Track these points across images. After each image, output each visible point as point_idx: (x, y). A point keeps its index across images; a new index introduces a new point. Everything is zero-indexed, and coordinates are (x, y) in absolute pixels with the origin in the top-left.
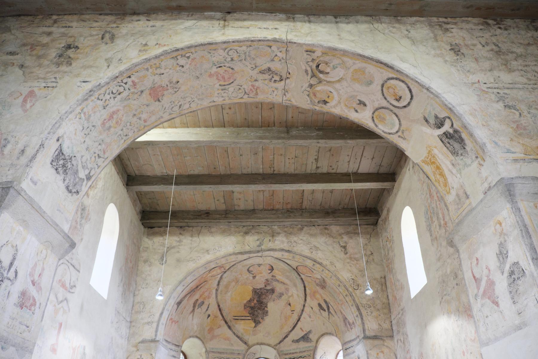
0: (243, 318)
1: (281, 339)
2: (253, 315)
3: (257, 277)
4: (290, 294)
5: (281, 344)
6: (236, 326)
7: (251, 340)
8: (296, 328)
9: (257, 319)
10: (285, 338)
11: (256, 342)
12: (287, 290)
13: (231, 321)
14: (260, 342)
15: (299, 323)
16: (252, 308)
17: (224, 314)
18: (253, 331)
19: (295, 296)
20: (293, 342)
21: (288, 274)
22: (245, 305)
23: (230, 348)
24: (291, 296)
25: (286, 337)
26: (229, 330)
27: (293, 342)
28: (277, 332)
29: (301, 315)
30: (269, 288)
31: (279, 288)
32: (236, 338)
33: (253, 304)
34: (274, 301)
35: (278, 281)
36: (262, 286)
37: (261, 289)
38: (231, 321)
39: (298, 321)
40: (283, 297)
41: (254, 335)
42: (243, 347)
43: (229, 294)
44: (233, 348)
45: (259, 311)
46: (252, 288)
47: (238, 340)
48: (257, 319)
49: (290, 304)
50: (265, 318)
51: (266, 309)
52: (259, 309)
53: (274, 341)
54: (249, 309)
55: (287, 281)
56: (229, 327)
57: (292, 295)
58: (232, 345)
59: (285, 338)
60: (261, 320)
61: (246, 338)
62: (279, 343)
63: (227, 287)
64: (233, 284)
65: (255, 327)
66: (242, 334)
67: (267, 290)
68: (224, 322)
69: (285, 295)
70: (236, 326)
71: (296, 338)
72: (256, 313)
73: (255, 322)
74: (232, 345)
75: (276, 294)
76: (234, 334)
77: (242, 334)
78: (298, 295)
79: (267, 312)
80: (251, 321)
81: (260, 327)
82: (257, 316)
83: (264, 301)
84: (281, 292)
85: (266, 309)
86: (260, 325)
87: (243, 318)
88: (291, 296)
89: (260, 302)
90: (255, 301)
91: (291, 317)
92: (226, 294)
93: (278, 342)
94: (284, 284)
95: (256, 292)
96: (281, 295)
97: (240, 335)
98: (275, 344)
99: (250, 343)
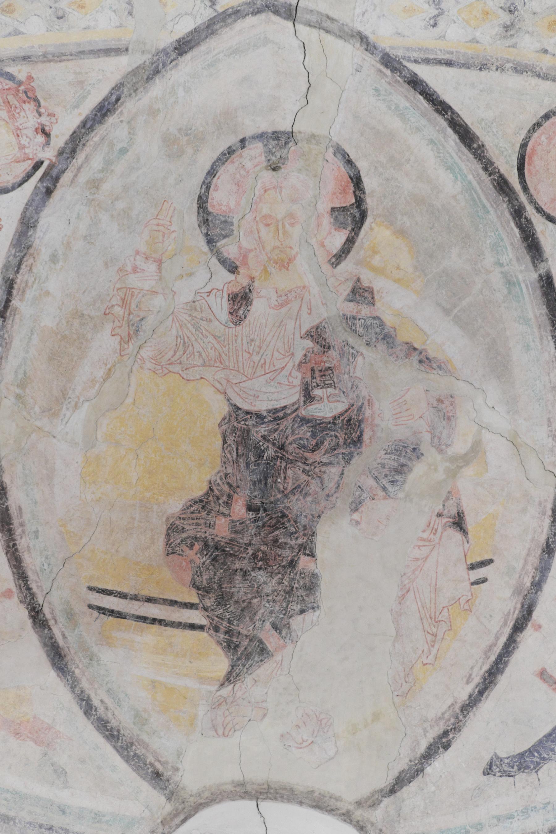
0: (153, 611)
1: (403, 764)
2: (223, 599)
3: (259, 307)
4: (460, 447)
5: (405, 792)
6: (107, 656)
7: (199, 763)
8: (503, 680)
9: (245, 628)
10: (429, 754)
11: (229, 774)
12: (444, 409)
13: (70, 615)
14: (257, 774)
15: (528, 638)
16: (218, 553)
17: (32, 562)
18: (217, 704)
19: (497, 450)
20: (488, 771)
21: (455, 260)
22: (173, 529)
23: (42, 790)
24: (465, 460)
25: (442, 743)
26: (52, 675)
27: (488, 771)
28: (376, 717)
29: (537, 585)
30: (326, 408)
31: (393, 399)
32: (98, 739)
33: (221, 529)
34: (356, 506)
35: (387, 338)
36: (290, 396)
37: (278, 415)
38: (70, 615)
39: (519, 627)
40: (418, 470)
41: (223, 730)
42: (143, 801)
43: (76, 421)
44: (64, 796)
45: (261, 576)
46: (221, 409)
47: (107, 748)
48: (245, 628)
49: (459, 522)
50: (296, 622)
51: (303, 562)
52: (261, 560)
53: (352, 776)
54: (195, 556)
55: (444, 338)
56: (57, 656)
57: (477, 449)
58: (61, 773)
59: (429, 754)
60: (271, 640)
61: (163, 744)
62: (393, 791)
63: (65, 348)
64: (104, 343)
65: (230, 678)
66: (141, 719)
67: (319, 427)
68: (23, 613)
69: (431, 454)
70: (107, 656)
71: (510, 746)
72: (240, 589)
73: (230, 646)
74: (61, 773)
75: (372, 453)
76: (88, 709)
77: (141, 719)
78: (514, 442)
79: (311, 585)
80: (203, 635)
81: (263, 682)
82: (247, 609)
83: (296, 505)
84: (401, 433)
85: (303, 562)
86: (264, 670)
87: (153, 611)
88: (465, 460)
89: (272, 518)
90: (239, 509)
91: (468, 608)
92: (52, 411)
93: (384, 780)
94: (426, 361)
95: (245, 435)
96: (405, 455)
97: (122, 718)
98: (365, 789)
99: (190, 780)
